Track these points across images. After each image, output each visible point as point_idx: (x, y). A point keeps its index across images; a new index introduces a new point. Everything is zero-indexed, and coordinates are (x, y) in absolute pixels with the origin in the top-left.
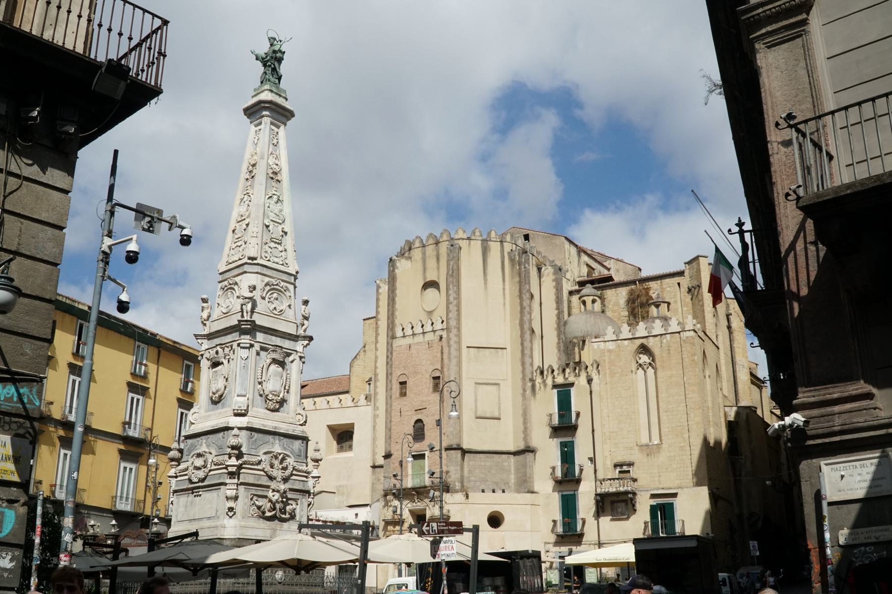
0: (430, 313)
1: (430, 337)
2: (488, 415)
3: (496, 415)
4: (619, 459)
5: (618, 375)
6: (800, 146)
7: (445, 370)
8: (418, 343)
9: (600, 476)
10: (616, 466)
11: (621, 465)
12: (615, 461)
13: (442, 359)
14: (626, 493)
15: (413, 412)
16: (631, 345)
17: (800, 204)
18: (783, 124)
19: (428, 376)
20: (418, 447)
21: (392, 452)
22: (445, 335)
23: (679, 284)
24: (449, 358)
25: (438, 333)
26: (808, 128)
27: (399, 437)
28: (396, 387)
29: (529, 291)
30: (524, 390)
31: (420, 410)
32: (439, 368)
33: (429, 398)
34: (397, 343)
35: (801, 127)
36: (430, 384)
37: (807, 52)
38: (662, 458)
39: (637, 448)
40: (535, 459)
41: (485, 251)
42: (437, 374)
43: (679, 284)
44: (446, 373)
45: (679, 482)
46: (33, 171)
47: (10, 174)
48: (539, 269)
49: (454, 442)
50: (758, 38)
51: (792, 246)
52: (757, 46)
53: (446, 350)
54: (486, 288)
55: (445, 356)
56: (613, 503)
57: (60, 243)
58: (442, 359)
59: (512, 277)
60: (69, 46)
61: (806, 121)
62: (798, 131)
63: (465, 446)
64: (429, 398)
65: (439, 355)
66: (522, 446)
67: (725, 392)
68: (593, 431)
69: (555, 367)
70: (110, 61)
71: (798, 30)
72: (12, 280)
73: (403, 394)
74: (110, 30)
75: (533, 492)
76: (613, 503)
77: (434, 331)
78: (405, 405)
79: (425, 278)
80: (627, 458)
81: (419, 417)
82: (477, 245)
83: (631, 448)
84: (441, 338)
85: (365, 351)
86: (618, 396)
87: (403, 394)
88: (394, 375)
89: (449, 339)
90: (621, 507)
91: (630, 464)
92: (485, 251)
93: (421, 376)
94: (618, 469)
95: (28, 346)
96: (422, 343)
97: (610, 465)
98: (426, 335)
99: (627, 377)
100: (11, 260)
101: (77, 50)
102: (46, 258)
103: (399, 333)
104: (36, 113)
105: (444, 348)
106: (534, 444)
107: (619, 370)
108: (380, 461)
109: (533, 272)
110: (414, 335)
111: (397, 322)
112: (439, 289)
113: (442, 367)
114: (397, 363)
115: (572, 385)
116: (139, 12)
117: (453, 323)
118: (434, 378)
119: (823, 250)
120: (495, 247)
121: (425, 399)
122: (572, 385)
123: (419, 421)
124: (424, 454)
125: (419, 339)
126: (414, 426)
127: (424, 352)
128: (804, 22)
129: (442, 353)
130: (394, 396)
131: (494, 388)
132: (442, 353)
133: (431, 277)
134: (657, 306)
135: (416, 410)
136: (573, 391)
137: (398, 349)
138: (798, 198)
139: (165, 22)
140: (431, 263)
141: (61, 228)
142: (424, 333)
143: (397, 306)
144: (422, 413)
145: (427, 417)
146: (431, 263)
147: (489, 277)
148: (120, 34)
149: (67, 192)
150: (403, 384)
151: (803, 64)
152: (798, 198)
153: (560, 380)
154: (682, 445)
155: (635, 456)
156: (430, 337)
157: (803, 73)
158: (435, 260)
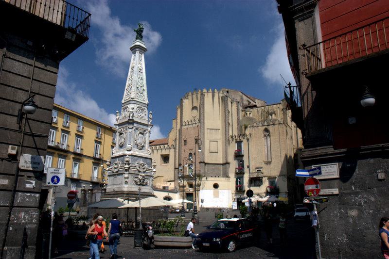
0: (195, 117)
1: (194, 125)
2: (214, 151)
3: (216, 151)
4: (258, 166)
6: (308, 57)
9: (251, 171)
14: (260, 177)
17: (307, 76)
18: (302, 48)
19: (193, 138)
24: (201, 133)
25: (197, 124)
26: (311, 50)
29: (228, 110)
30: (226, 143)
34: (183, 127)
35: (308, 49)
36: (194, 141)
37: (313, 23)
38: (272, 165)
41: (213, 96)
46: (42, 66)
47: (35, 67)
48: (232, 103)
49: (202, 161)
50: (296, 18)
51: (306, 92)
52: (295, 21)
53: (200, 130)
54: (214, 109)
56: (255, 181)
57: (54, 91)
59: (222, 104)
60: (54, 21)
61: (309, 47)
62: (307, 50)
63: (206, 162)
66: (225, 162)
67: (294, 144)
69: (237, 135)
70: (69, 27)
71: (310, 14)
72: (35, 103)
73: (185, 144)
74: (70, 17)
75: (228, 177)
76: (255, 181)
80: (260, 166)
82: (210, 94)
87: (185, 144)
89: (201, 126)
90: (258, 182)
91: (261, 168)
92: (213, 96)
94: (257, 169)
95: (43, 126)
97: (254, 168)
100: (34, 96)
101: (57, 24)
102: (49, 96)
103: (184, 124)
104: (44, 46)
108: (177, 167)
109: (230, 103)
111: (183, 120)
112: (197, 110)
116: (80, 11)
118: (196, 139)
119: (314, 93)
120: (216, 95)
122: (242, 141)
125: (191, 126)
128: (313, 11)
131: (216, 142)
133: (195, 105)
134: (271, 115)
136: (242, 144)
138: (306, 74)
139: (90, 15)
141: (55, 86)
142: (192, 124)
143: (183, 115)
146: (195, 100)
147: (214, 104)
148: (73, 19)
149: (56, 73)
150: (185, 141)
151: (311, 27)
152: (306, 74)
157: (311, 30)
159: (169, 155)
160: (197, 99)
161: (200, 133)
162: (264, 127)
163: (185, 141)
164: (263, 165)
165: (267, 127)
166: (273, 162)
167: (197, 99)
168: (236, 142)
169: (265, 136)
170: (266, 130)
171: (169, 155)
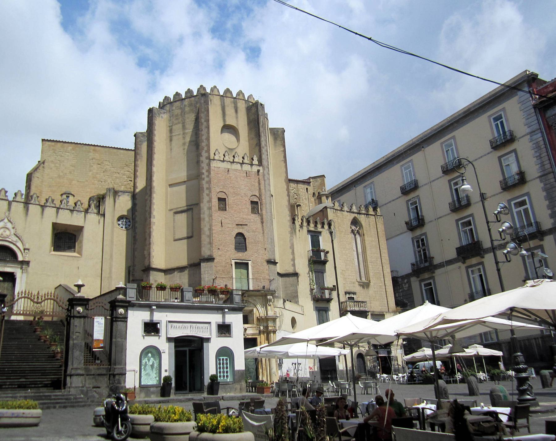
5: (343, 233)
7: (263, 198)
8: (236, 170)
10: (346, 293)
11: (349, 293)
12: (345, 290)
13: (260, 189)
15: (234, 226)
16: (349, 216)
19: (247, 199)
20: (241, 256)
21: (214, 256)
22: (261, 171)
23: (307, 189)
27: (221, 244)
28: (215, 202)
31: (241, 225)
32: (258, 195)
33: (249, 217)
39: (357, 283)
40: (298, 281)
42: (256, 200)
43: (307, 189)
44: (264, 201)
45: (380, 308)
53: (262, 182)
55: (262, 187)
58: (260, 189)
64: (249, 217)
65: (257, 184)
66: (291, 270)
68: (335, 267)
77: (252, 165)
78: (225, 217)
79: (224, 120)
80: (353, 290)
81: (241, 231)
83: (354, 283)
84: (258, 171)
85: (43, 167)
86: (344, 247)
88: (213, 190)
93: (241, 197)
94: (348, 296)
96: (239, 170)
98: (244, 165)
99: (348, 236)
105: (261, 181)
106: (298, 271)
107: (344, 231)
110: (233, 162)
113: (260, 195)
114: (215, 181)
115: (320, 233)
117: (264, 162)
118: (252, 202)
121: (245, 217)
123: (240, 235)
124: (247, 264)
126: (235, 238)
127: (242, 178)
129: (259, 184)
130: (213, 208)
132: (259, 184)
135: (237, 225)
136: (321, 238)
137: (215, 169)
140: (230, 111)
144: (243, 228)
145: (249, 233)
150: (222, 201)
153: (312, 227)
154: (381, 285)
155: (357, 288)
156: (246, 168)
158: (233, 111)
159: (83, 227)
160: (236, 111)
161: (263, 191)
162: (353, 215)
163: (222, 201)
164: (357, 288)
165: (356, 215)
166: (371, 284)
167: (236, 111)
168: (309, 231)
169: (353, 231)
170: (355, 222)
171: (83, 227)
